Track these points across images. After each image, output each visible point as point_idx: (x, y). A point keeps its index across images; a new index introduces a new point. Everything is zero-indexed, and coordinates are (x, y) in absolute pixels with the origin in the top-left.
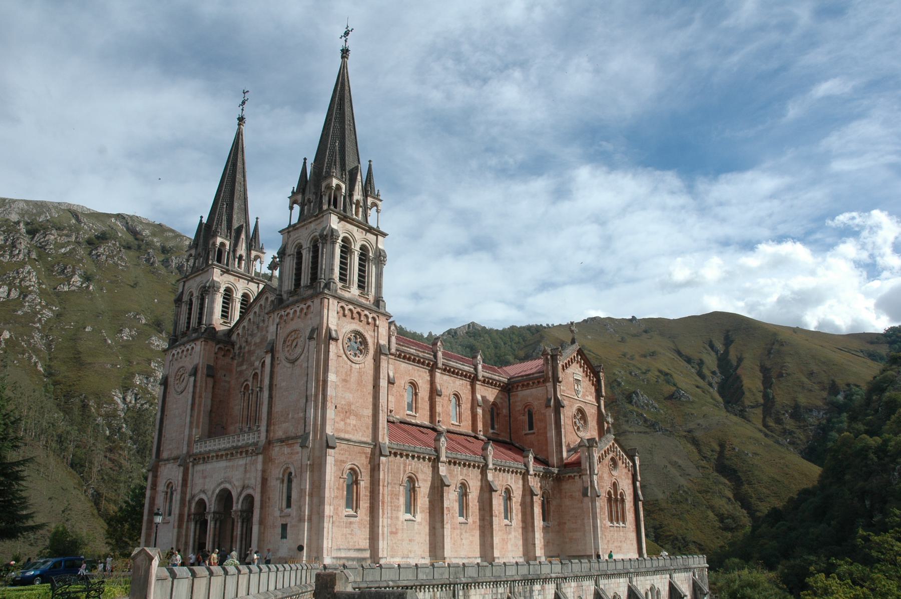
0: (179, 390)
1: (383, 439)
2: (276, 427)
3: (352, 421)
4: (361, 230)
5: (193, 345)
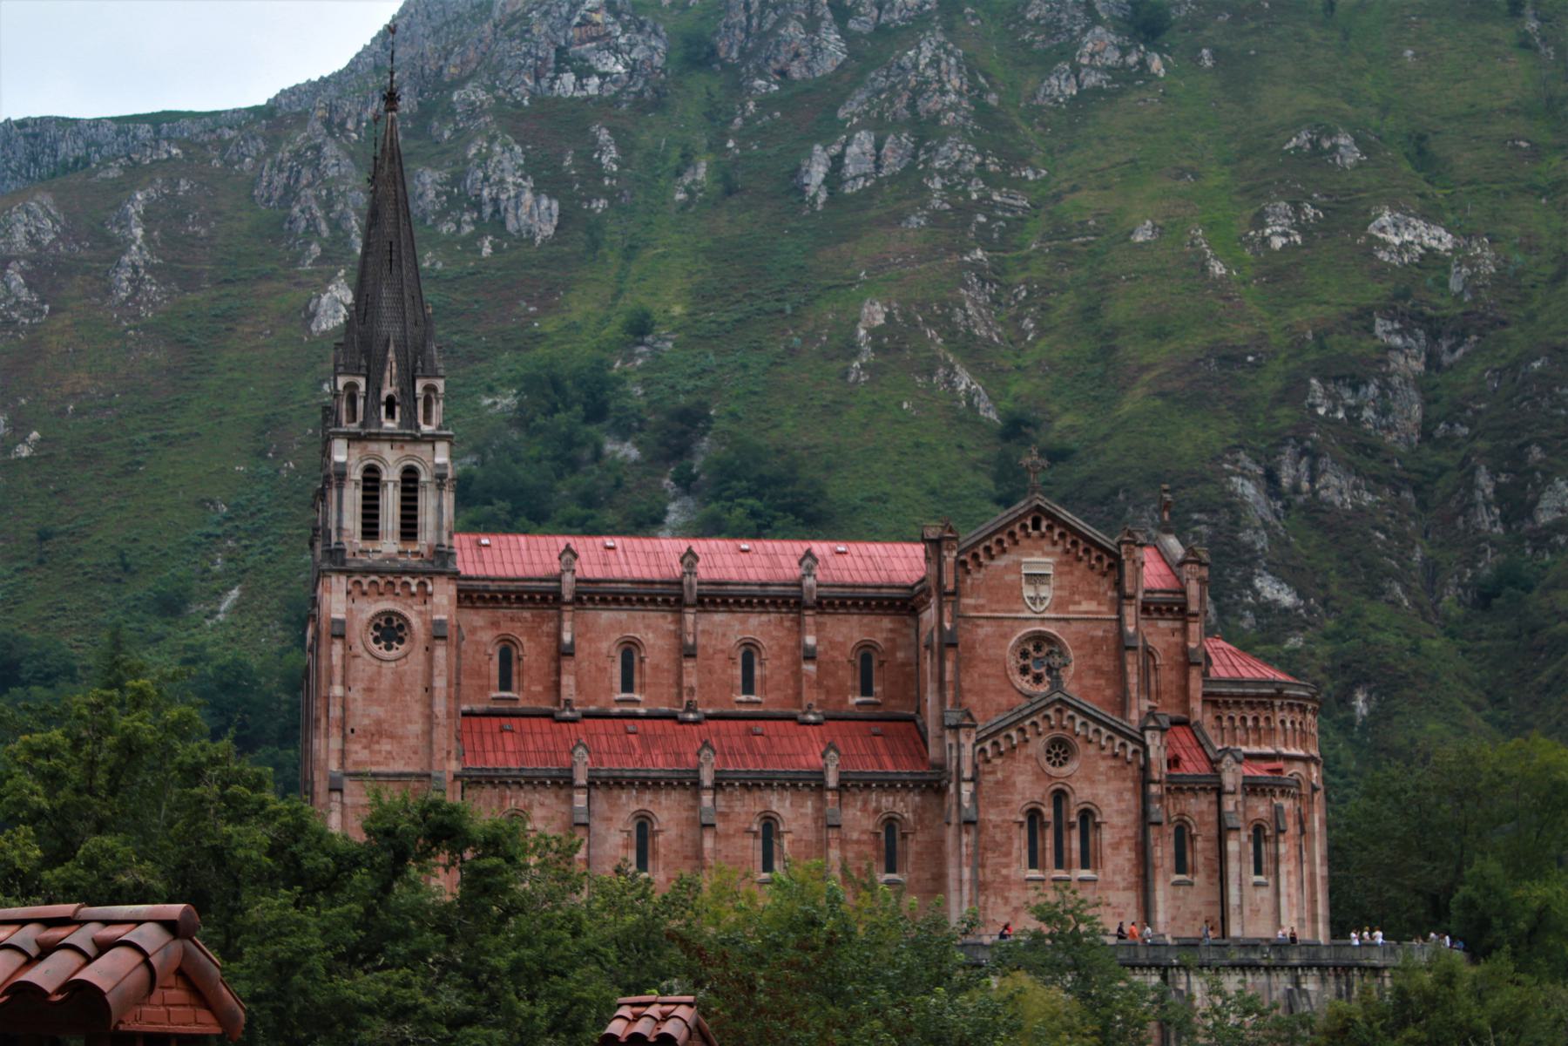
3: (386, 746)
4: (398, 444)
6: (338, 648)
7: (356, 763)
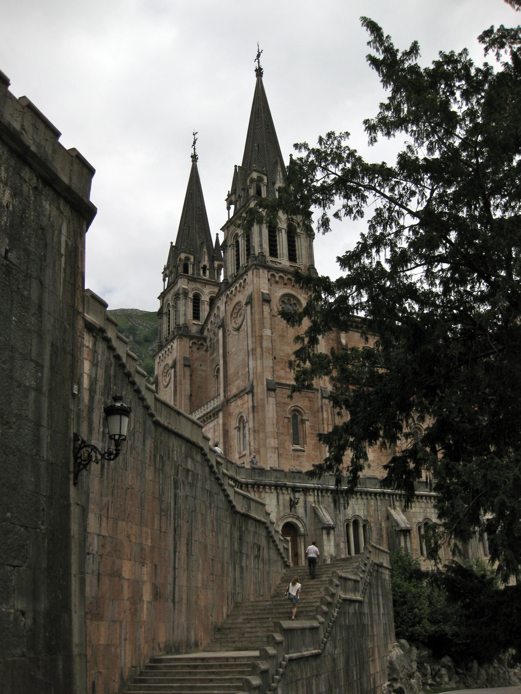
0: (166, 384)
1: (325, 384)
2: (232, 386)
5: (172, 344)
6: (266, 308)
7: (278, 377)
